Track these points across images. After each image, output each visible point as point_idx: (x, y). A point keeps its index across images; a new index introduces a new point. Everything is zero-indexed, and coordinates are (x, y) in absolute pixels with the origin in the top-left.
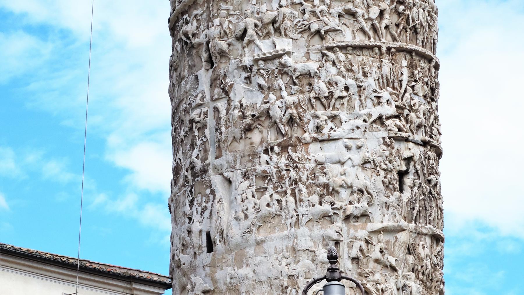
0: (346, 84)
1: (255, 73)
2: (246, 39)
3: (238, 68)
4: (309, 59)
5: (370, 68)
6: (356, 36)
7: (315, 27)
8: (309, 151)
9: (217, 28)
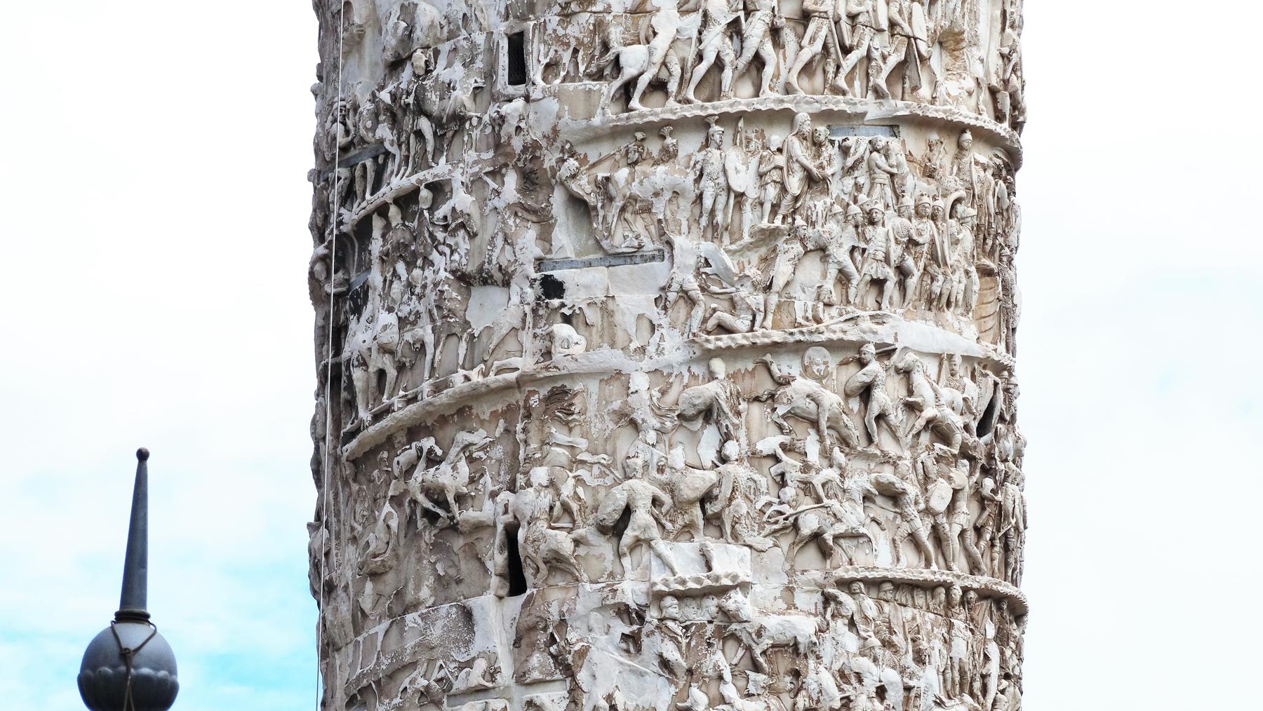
0: (880, 681)
1: (652, 628)
2: (629, 535)
3: (603, 608)
4: (791, 606)
5: (929, 641)
6: (901, 554)
7: (809, 524)
9: (542, 494)
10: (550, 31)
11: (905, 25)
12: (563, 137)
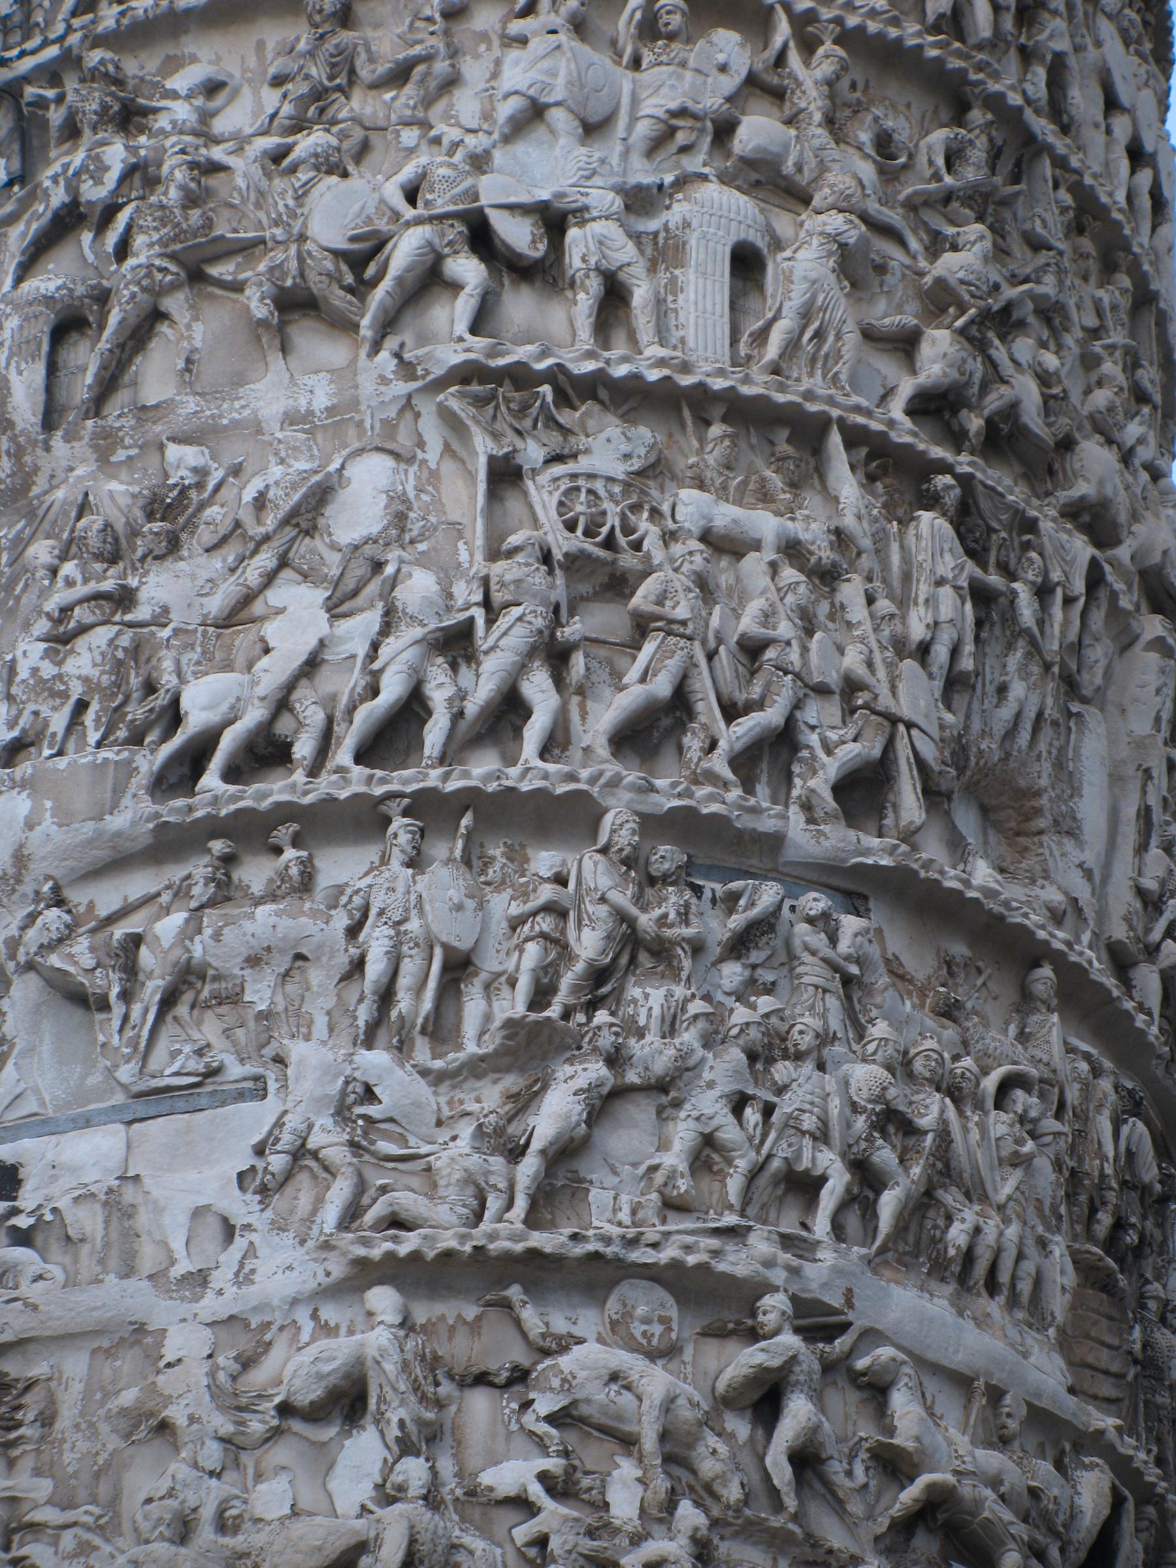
10: (23, 673)
11: (884, 690)
12: (37, 868)
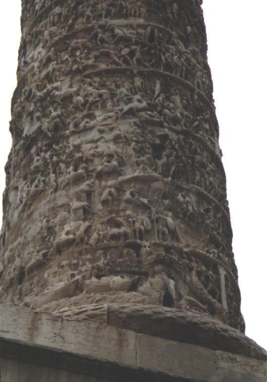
7: (75, 67)
8: (69, 141)
